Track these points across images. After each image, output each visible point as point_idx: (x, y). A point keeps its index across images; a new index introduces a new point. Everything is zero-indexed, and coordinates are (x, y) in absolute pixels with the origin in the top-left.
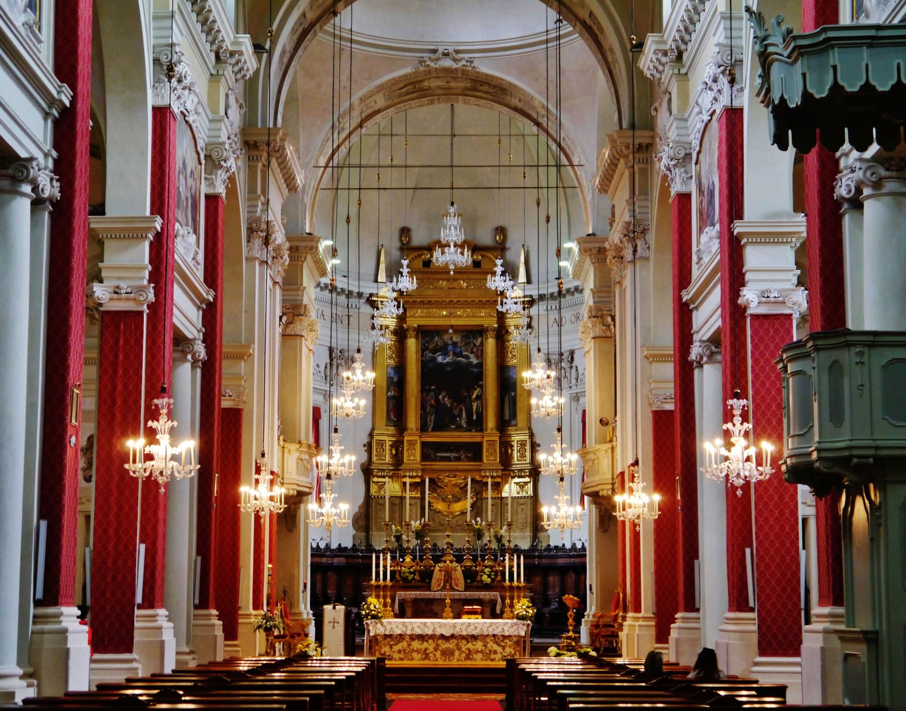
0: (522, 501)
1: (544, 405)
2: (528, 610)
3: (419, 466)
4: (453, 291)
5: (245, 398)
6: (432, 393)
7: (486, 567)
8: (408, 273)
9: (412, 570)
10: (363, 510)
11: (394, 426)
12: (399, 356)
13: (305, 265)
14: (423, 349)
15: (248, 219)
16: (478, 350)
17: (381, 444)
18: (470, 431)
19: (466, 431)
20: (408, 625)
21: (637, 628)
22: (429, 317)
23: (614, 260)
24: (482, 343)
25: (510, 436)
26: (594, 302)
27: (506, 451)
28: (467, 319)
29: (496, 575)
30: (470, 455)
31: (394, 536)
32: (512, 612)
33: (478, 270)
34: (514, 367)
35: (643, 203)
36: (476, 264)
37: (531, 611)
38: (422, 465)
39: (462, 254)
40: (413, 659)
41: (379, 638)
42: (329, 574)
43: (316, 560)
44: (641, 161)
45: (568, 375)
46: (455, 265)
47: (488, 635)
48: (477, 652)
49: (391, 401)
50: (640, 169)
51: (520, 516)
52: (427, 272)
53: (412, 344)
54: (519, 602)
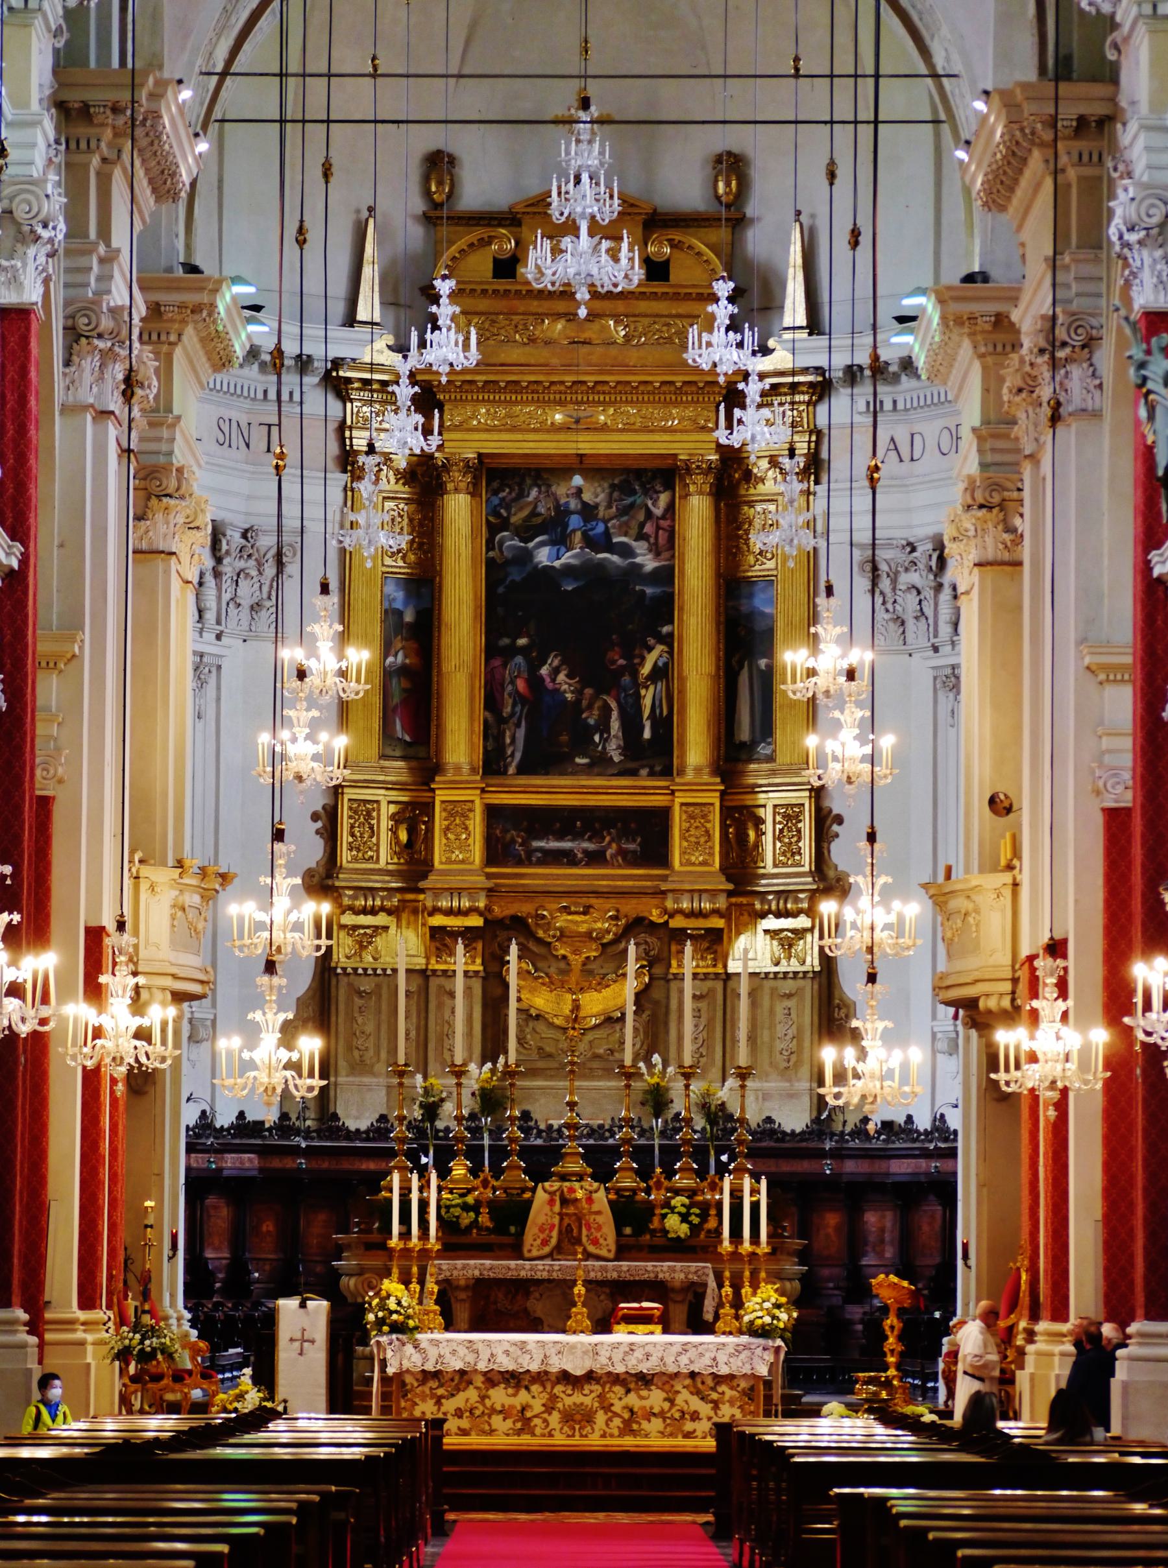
0: (789, 986)
1: (839, 754)
2: (776, 1312)
3: (480, 881)
4: (584, 349)
5: (60, 770)
6: (519, 659)
7: (677, 1192)
8: (453, 318)
9: (470, 1199)
11: (403, 758)
12: (421, 545)
13: (178, 352)
14: (495, 525)
15: (67, 304)
16: (658, 528)
17: (365, 811)
18: (633, 773)
19: (623, 773)
20: (480, 1347)
21: (1057, 1359)
22: (514, 429)
23: (1018, 399)
24: (671, 508)
25: (752, 790)
26: (983, 466)
27: (742, 837)
28: (624, 437)
29: (704, 1216)
30: (632, 847)
31: (421, 1106)
32: (738, 1317)
33: (658, 288)
34: (769, 582)
35: (1088, 270)
36: (656, 270)
37: (784, 1316)
38: (489, 876)
39: (614, 256)
40: (492, 1432)
41: (408, 1379)
42: (211, 1200)
44: (1085, 158)
45: (929, 610)
46: (595, 295)
47: (677, 1375)
48: (650, 1415)
49: (394, 681)
50: (1080, 179)
51: (780, 1030)
52: (507, 292)
54: (754, 1294)
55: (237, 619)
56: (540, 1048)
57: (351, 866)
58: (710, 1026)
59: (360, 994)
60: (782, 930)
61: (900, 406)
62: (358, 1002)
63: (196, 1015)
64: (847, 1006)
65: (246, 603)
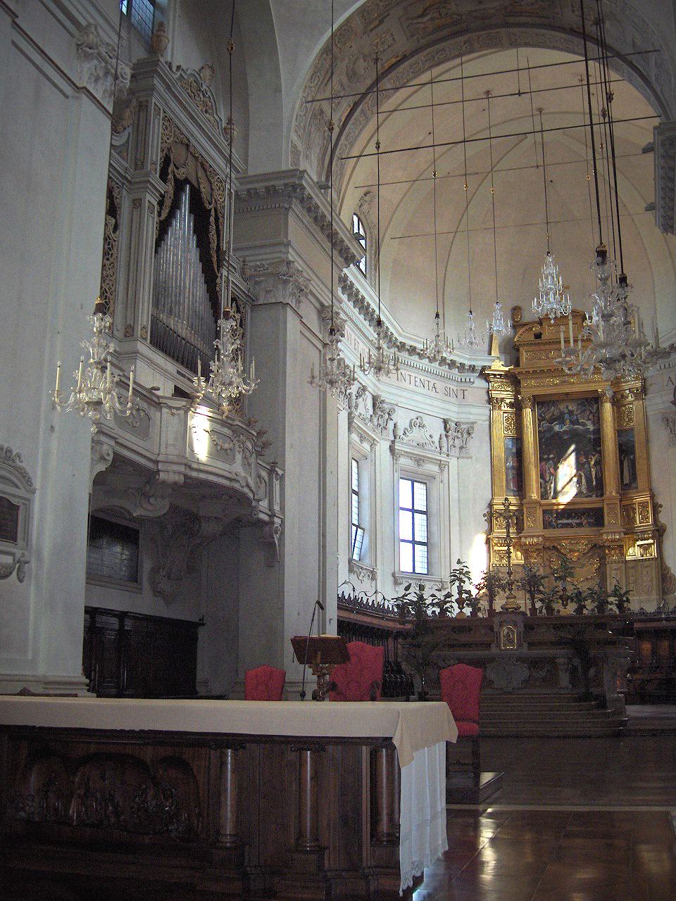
11: (514, 496)
16: (594, 416)
25: (632, 499)
27: (628, 516)
43: (345, 614)
51: (645, 579)
53: (528, 414)
55: (455, 452)
61: (671, 366)
65: (458, 446)
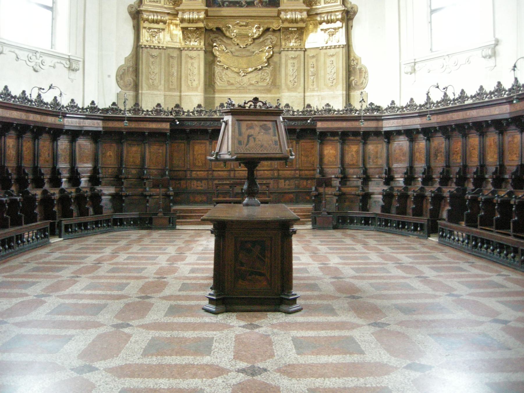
10: (131, 64)
51: (329, 70)
56: (228, 81)
57: (148, 3)
58: (298, 70)
59: (152, 56)
60: (329, 29)
62: (152, 60)
63: (71, 57)
64: (357, 60)
